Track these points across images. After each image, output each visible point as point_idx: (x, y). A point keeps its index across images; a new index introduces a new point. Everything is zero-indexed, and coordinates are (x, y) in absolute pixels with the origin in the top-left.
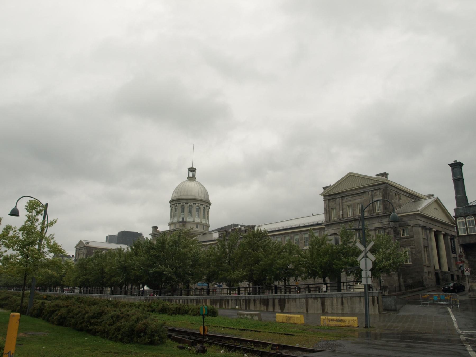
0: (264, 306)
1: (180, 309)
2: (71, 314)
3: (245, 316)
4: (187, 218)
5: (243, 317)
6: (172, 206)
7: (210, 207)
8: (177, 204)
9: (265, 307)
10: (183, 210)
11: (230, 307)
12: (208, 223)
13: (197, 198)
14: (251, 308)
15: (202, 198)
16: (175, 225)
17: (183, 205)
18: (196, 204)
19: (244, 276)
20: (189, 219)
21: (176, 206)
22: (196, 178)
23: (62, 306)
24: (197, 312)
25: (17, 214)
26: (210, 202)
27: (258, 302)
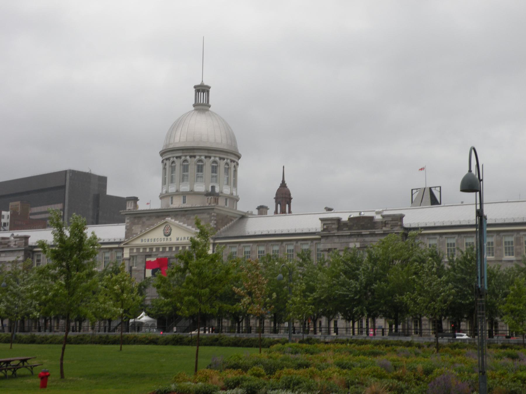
4: (195, 185)
6: (165, 161)
8: (175, 159)
13: (214, 146)
16: (172, 198)
17: (185, 161)
21: (173, 162)
22: (210, 106)
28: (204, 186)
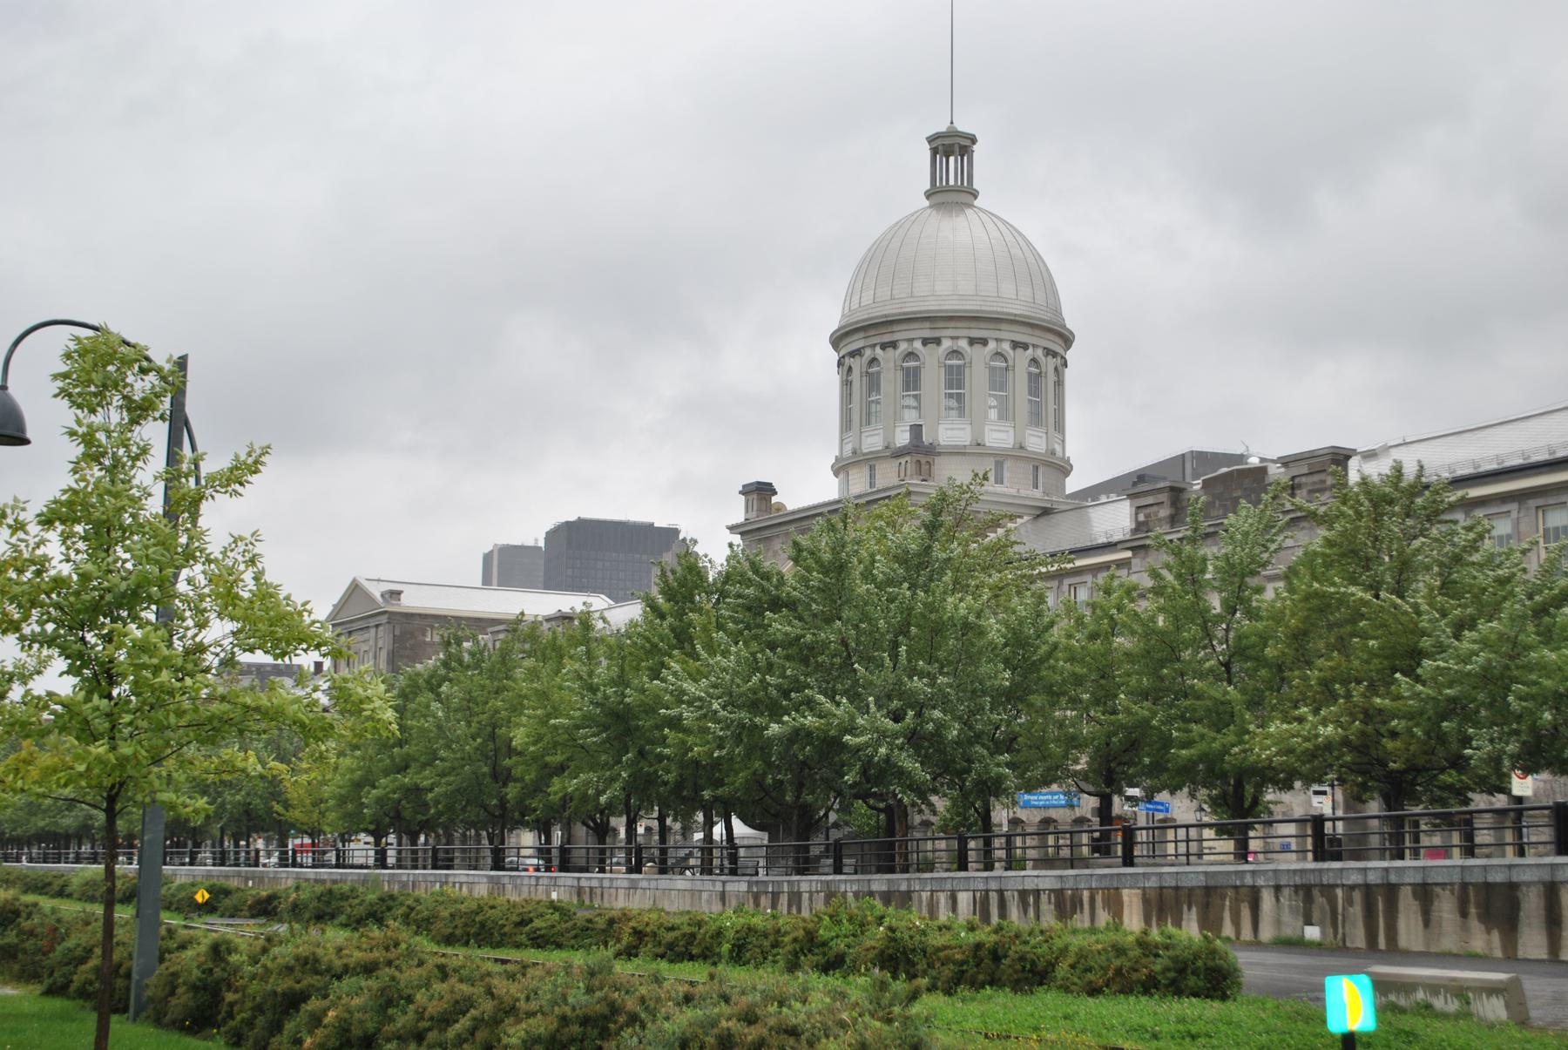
0: (1488, 932)
1: (996, 955)
2: (403, 1020)
3: (1420, 995)
4: (941, 428)
5: (1402, 1002)
6: (847, 361)
7: (1070, 355)
8: (878, 350)
9: (1496, 936)
10: (912, 380)
11: (1266, 934)
12: (1058, 448)
14: (1403, 941)
15: (1016, 309)
16: (872, 468)
17: (911, 355)
18: (984, 342)
19: (1328, 746)
20: (951, 433)
22: (975, 195)
23: (338, 963)
24: (1110, 974)
25: (16, 434)
26: (1064, 326)
27: (1446, 908)
28: (968, 428)
